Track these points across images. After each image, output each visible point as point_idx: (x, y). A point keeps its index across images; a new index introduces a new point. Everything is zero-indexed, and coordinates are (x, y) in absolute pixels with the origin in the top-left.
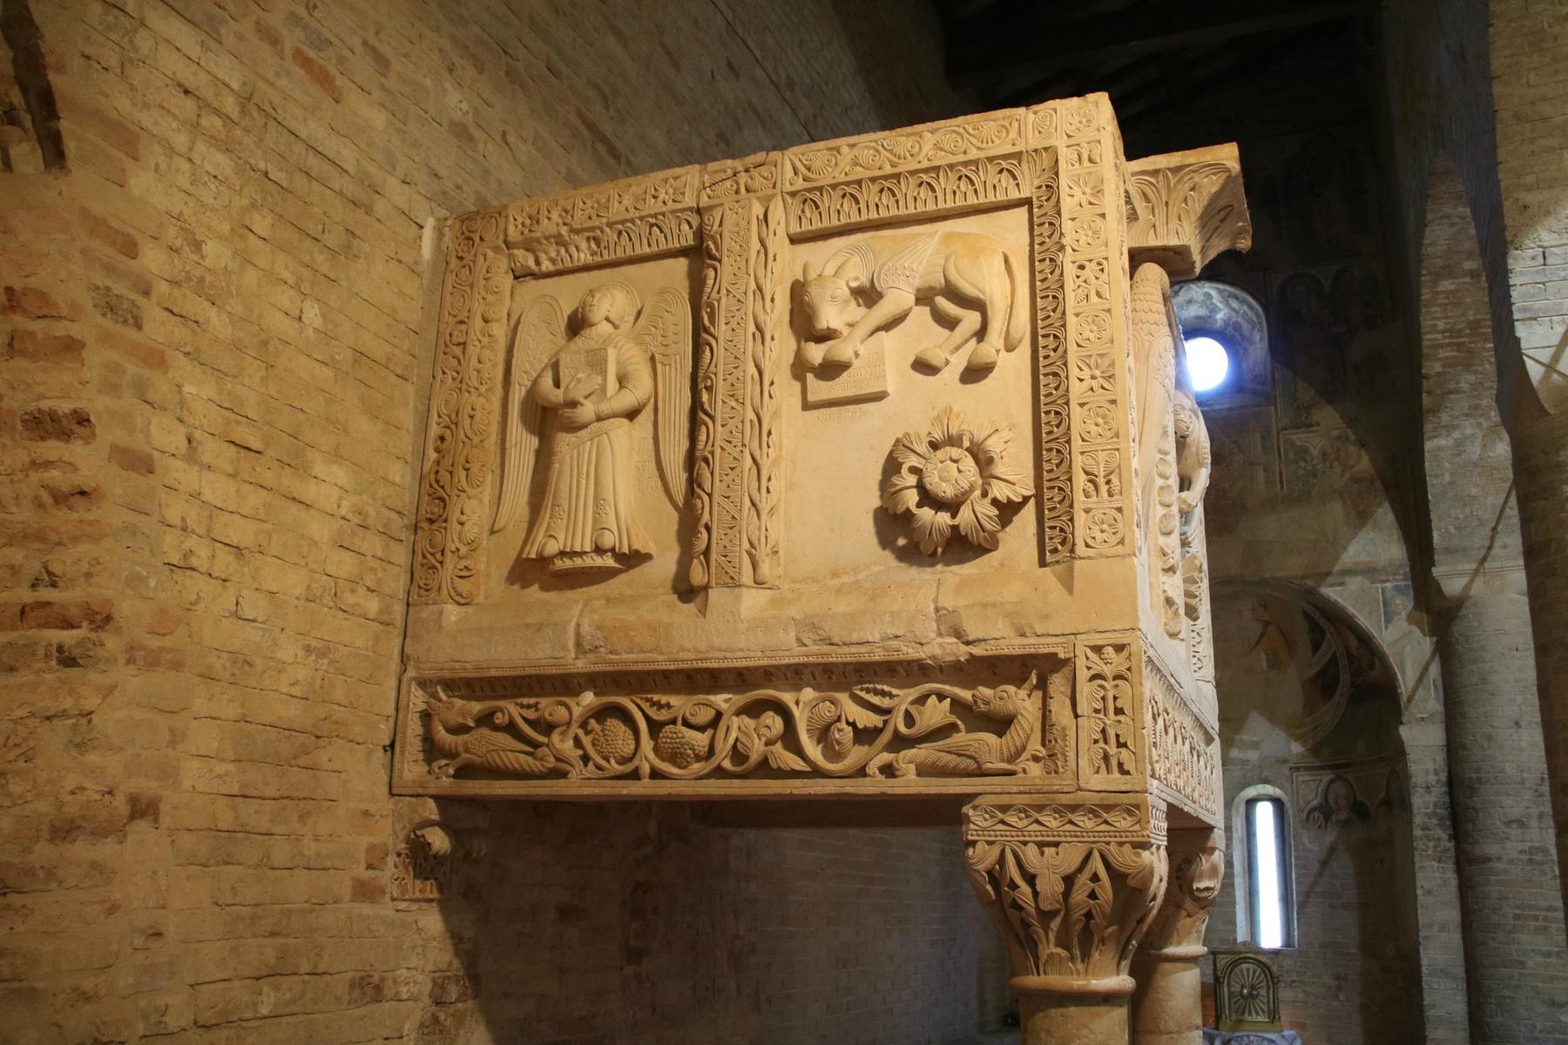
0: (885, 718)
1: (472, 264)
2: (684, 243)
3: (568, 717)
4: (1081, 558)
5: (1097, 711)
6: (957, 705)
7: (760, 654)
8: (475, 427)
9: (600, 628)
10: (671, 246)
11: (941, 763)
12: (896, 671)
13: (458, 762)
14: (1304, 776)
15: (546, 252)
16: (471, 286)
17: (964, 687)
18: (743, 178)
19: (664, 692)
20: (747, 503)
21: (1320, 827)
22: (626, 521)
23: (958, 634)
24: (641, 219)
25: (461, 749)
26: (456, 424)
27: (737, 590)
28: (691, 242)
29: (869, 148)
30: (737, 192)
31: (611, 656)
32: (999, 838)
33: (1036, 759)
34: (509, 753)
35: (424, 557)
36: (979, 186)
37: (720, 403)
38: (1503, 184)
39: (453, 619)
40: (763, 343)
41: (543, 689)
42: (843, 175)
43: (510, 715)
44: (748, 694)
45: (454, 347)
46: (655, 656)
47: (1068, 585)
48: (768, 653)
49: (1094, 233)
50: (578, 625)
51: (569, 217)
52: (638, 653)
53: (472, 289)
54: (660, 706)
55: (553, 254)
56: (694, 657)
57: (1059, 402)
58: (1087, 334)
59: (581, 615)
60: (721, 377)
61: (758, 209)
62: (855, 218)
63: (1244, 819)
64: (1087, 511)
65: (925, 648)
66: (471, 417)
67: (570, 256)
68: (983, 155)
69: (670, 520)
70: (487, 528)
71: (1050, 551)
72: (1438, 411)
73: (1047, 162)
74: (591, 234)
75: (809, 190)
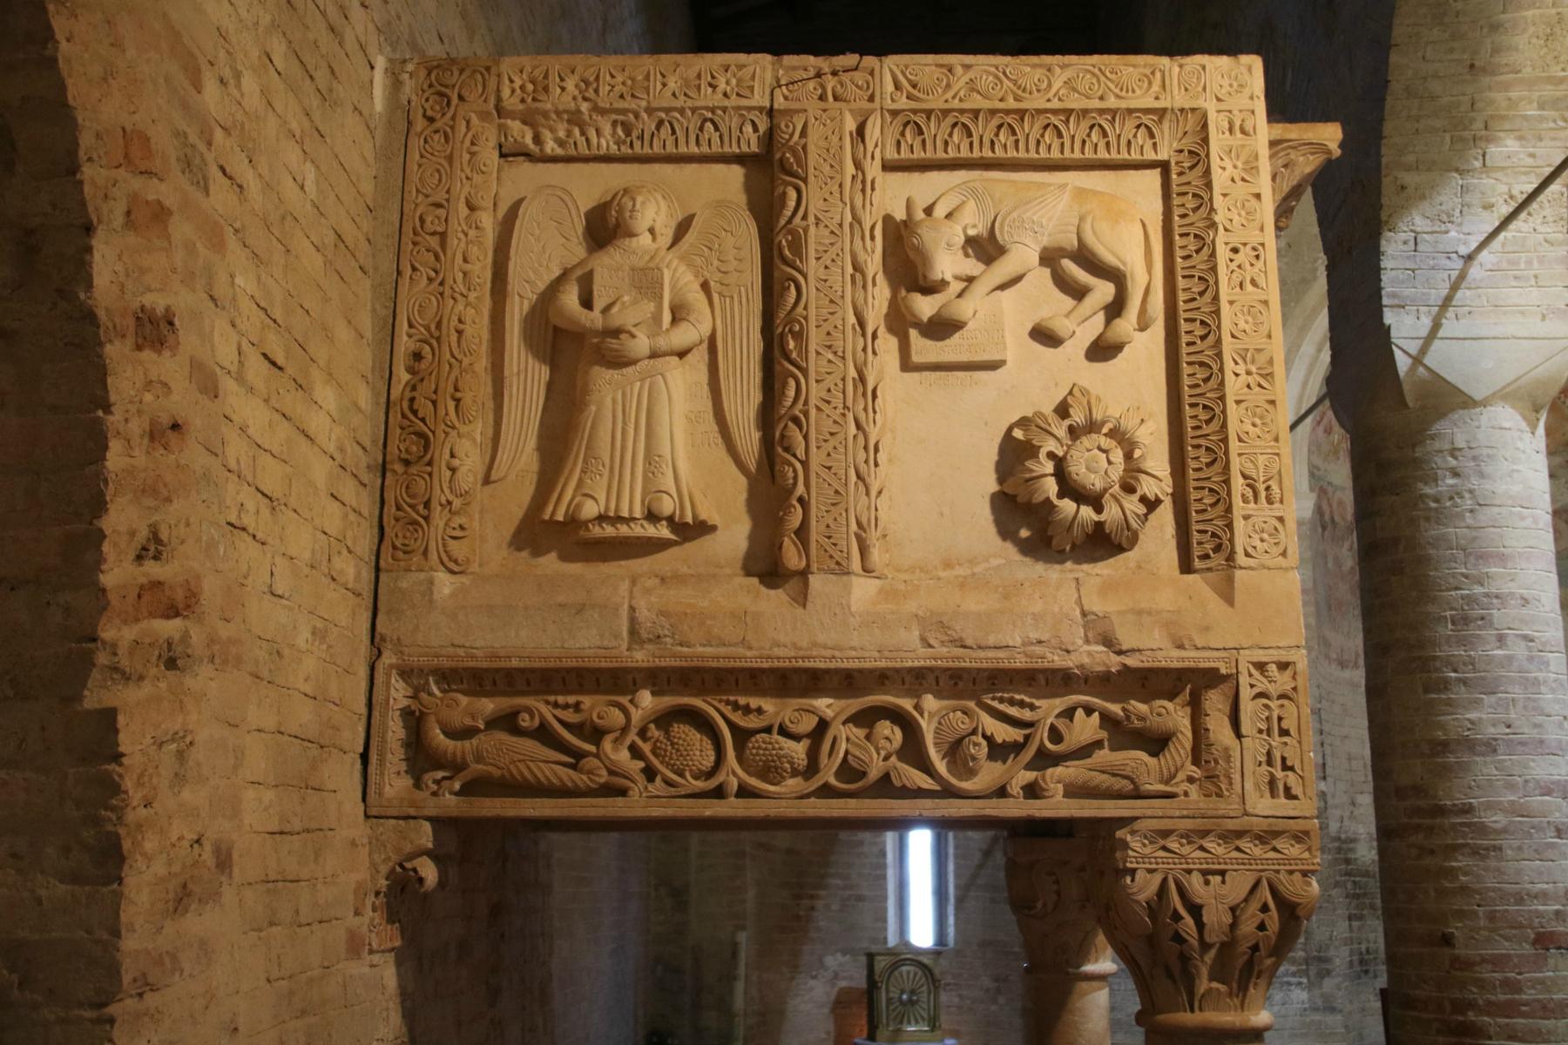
0: (1027, 731)
1: (448, 130)
2: (745, 149)
3: (624, 721)
4: (1241, 568)
5: (1260, 731)
6: (1107, 720)
7: (877, 655)
8: (464, 344)
9: (662, 613)
10: (727, 149)
11: (1093, 784)
12: (1034, 680)
13: (466, 775)
15: (552, 130)
16: (450, 159)
17: (1114, 701)
18: (831, 83)
19: (747, 692)
20: (853, 477)
22: (688, 485)
23: (1108, 642)
24: (694, 110)
25: (470, 758)
26: (438, 339)
27: (845, 578)
28: (755, 148)
29: (989, 73)
30: (822, 98)
31: (679, 648)
32: (1161, 866)
33: (1191, 780)
34: (541, 764)
35: (399, 508)
36: (1112, 138)
37: (812, 355)
38: (1384, 160)
39: (447, 591)
40: (864, 287)
41: (581, 685)
42: (957, 101)
43: (541, 714)
44: (861, 700)
45: (428, 237)
46: (741, 651)
47: (1227, 593)
48: (886, 654)
49: (1247, 213)
50: (632, 609)
51: (591, 90)
52: (717, 646)
53: (451, 165)
54: (747, 710)
55: (562, 134)
56: (793, 654)
57: (1208, 395)
58: (1242, 325)
59: (631, 597)
60: (813, 322)
61: (850, 125)
62: (965, 153)
64: (1246, 518)
65: (1073, 656)
66: (460, 332)
67: (587, 140)
68: (1124, 105)
69: (738, 486)
70: (480, 477)
71: (1199, 557)
73: (1191, 123)
74: (621, 118)
75: (915, 112)
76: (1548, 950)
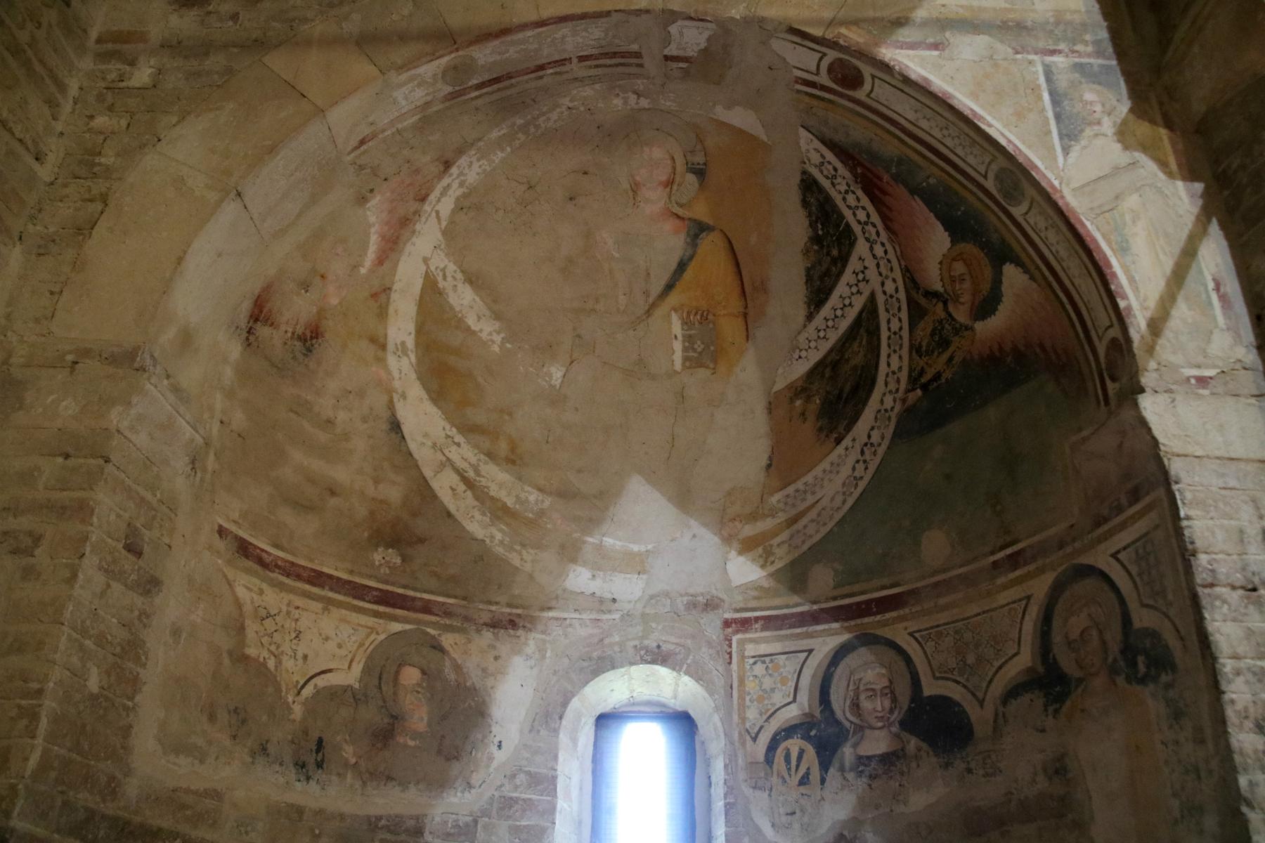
14: (758, 643)
21: (804, 781)
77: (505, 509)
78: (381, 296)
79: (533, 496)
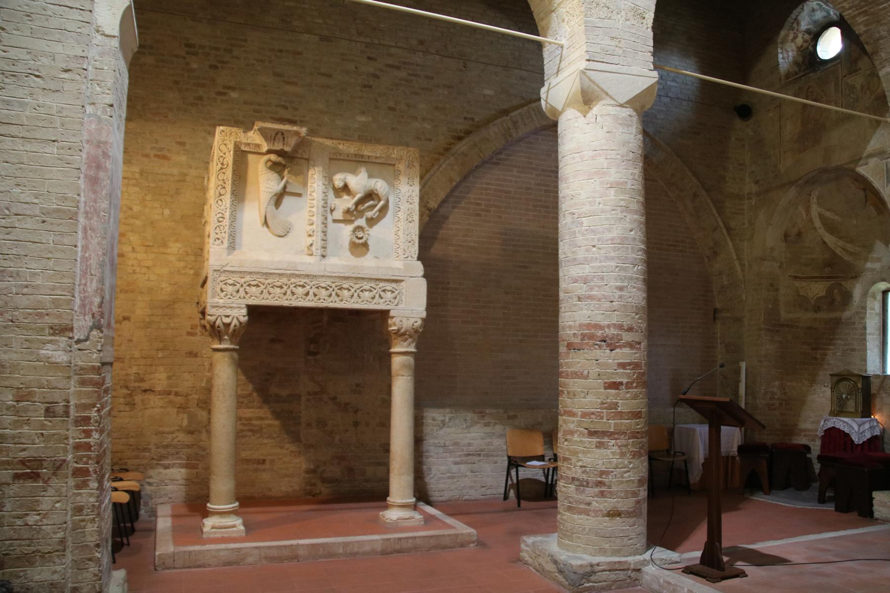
63: (881, 302)
72: (877, 52)
76: (570, 350)
77: (852, 253)
78: (811, 220)
79: (857, 249)
